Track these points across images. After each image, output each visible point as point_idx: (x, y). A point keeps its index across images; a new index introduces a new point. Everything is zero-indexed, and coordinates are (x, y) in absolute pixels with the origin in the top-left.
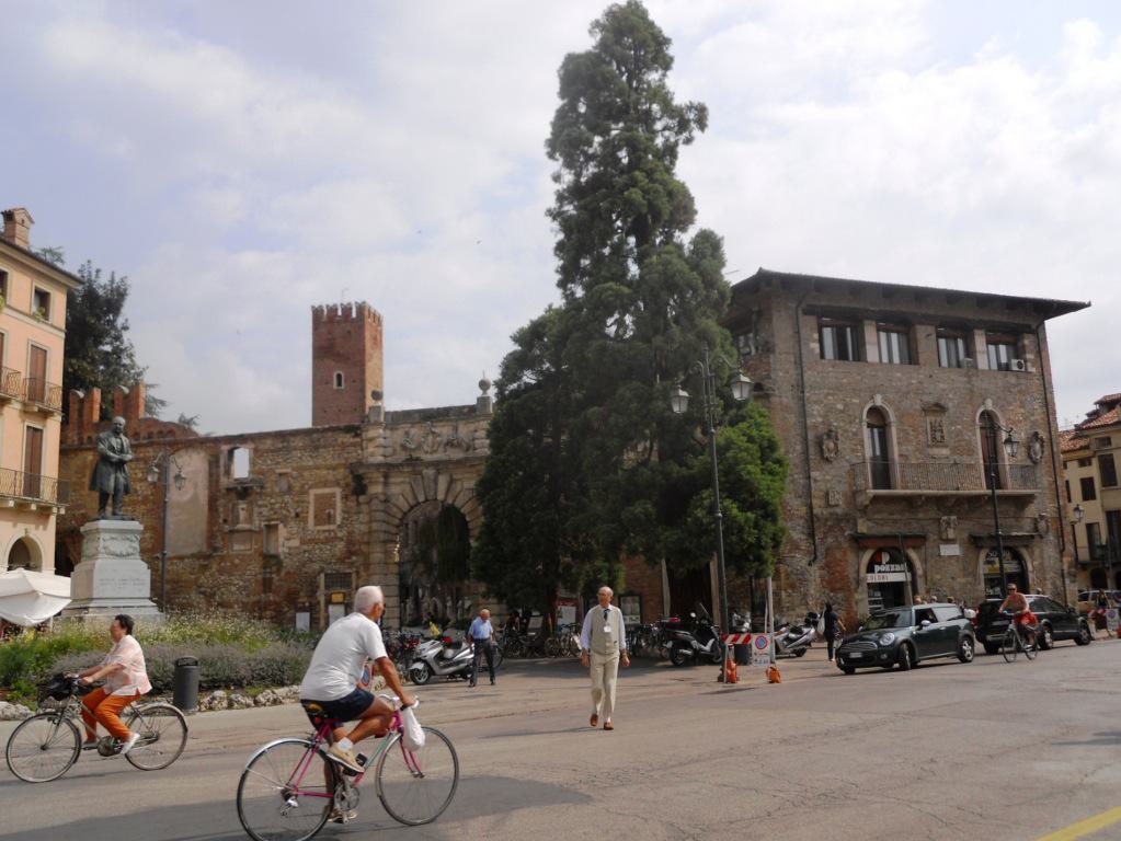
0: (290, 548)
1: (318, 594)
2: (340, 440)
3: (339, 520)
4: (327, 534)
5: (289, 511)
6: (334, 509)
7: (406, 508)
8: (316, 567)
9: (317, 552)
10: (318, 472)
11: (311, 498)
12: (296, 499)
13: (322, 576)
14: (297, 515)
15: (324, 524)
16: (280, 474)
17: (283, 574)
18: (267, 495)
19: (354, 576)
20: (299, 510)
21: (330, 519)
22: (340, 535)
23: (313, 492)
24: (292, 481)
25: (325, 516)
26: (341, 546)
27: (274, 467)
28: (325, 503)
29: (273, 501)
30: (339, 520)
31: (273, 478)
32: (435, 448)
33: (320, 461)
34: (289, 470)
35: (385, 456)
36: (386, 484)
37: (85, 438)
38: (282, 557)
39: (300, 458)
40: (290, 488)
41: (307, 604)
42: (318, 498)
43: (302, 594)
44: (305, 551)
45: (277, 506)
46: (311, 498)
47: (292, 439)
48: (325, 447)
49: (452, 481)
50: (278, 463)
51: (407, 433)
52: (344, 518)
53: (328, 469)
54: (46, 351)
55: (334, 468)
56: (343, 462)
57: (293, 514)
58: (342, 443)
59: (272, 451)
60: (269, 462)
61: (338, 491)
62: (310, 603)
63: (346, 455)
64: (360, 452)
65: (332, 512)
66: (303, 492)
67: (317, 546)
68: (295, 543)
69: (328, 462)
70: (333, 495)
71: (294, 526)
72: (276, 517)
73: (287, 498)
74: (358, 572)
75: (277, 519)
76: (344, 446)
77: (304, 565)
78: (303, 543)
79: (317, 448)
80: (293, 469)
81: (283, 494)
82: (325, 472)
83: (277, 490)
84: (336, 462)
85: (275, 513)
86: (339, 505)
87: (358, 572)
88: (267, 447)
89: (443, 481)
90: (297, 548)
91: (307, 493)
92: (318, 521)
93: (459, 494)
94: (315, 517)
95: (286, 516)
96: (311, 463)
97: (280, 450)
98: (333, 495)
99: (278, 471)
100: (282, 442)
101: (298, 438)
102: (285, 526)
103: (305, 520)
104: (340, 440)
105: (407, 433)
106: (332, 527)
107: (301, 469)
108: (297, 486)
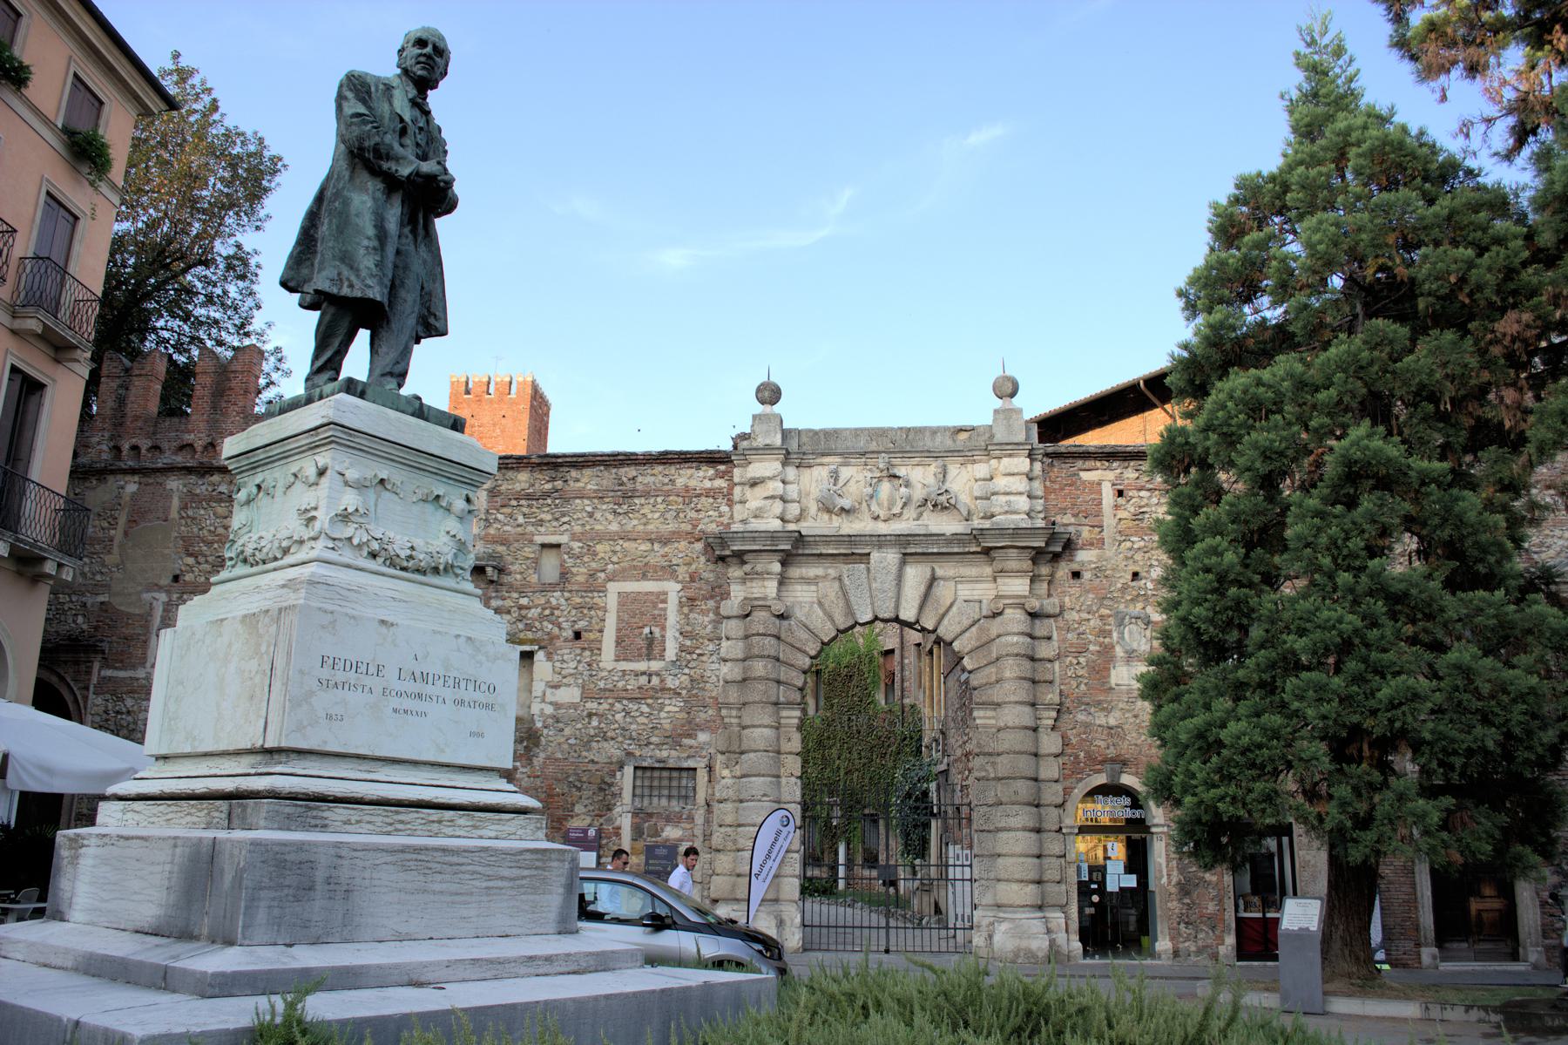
0: (557, 706)
1: (618, 809)
2: (680, 482)
3: (671, 652)
4: (643, 680)
5: (560, 628)
6: (663, 628)
7: (827, 633)
8: (612, 750)
9: (619, 717)
10: (626, 545)
11: (612, 601)
12: (578, 600)
13: (629, 770)
14: (578, 635)
15: (638, 657)
16: (544, 546)
17: (537, 762)
18: (511, 588)
19: (702, 776)
20: (581, 625)
21: (651, 648)
22: (671, 683)
23: (614, 588)
24: (570, 562)
25: (642, 643)
26: (673, 707)
27: (530, 528)
28: (640, 612)
29: (524, 601)
30: (671, 652)
31: (528, 551)
32: (896, 510)
33: (633, 523)
34: (564, 539)
35: (782, 520)
36: (783, 581)
37: (126, 446)
38: (539, 725)
39: (591, 515)
40: (565, 575)
41: (592, 832)
42: (624, 598)
43: (578, 808)
44: (590, 715)
45: (534, 613)
46: (612, 601)
47: (574, 473)
48: (646, 494)
49: (933, 580)
50: (541, 522)
51: (835, 476)
52: (682, 649)
53: (652, 541)
54: (76, 218)
55: (665, 541)
56: (689, 528)
57: (569, 634)
58: (687, 489)
59: (529, 497)
60: (521, 520)
61: (672, 588)
62: (599, 831)
63: (693, 514)
64: (724, 509)
65: (657, 631)
66: (593, 586)
67: (618, 706)
68: (570, 695)
69: (650, 527)
70: (662, 597)
71: (569, 657)
72: (530, 635)
73: (556, 598)
74: (710, 768)
75: (532, 642)
76: (689, 495)
77: (587, 745)
78: (586, 696)
79: (628, 496)
80: (574, 537)
81: (546, 588)
82: (645, 546)
83: (534, 578)
84: (672, 527)
85: (529, 627)
86: (673, 617)
87: (710, 768)
88: (518, 487)
89: (915, 575)
90: (575, 706)
91: (602, 590)
92: (624, 649)
93: (951, 605)
94: (618, 642)
95: (552, 638)
96: (614, 527)
97: (546, 495)
98: (662, 597)
99: (539, 539)
100: (553, 479)
101: (588, 472)
102: (549, 657)
103: (595, 648)
104: (680, 482)
105: (835, 476)
106: (655, 665)
107: (590, 539)
108: (580, 574)
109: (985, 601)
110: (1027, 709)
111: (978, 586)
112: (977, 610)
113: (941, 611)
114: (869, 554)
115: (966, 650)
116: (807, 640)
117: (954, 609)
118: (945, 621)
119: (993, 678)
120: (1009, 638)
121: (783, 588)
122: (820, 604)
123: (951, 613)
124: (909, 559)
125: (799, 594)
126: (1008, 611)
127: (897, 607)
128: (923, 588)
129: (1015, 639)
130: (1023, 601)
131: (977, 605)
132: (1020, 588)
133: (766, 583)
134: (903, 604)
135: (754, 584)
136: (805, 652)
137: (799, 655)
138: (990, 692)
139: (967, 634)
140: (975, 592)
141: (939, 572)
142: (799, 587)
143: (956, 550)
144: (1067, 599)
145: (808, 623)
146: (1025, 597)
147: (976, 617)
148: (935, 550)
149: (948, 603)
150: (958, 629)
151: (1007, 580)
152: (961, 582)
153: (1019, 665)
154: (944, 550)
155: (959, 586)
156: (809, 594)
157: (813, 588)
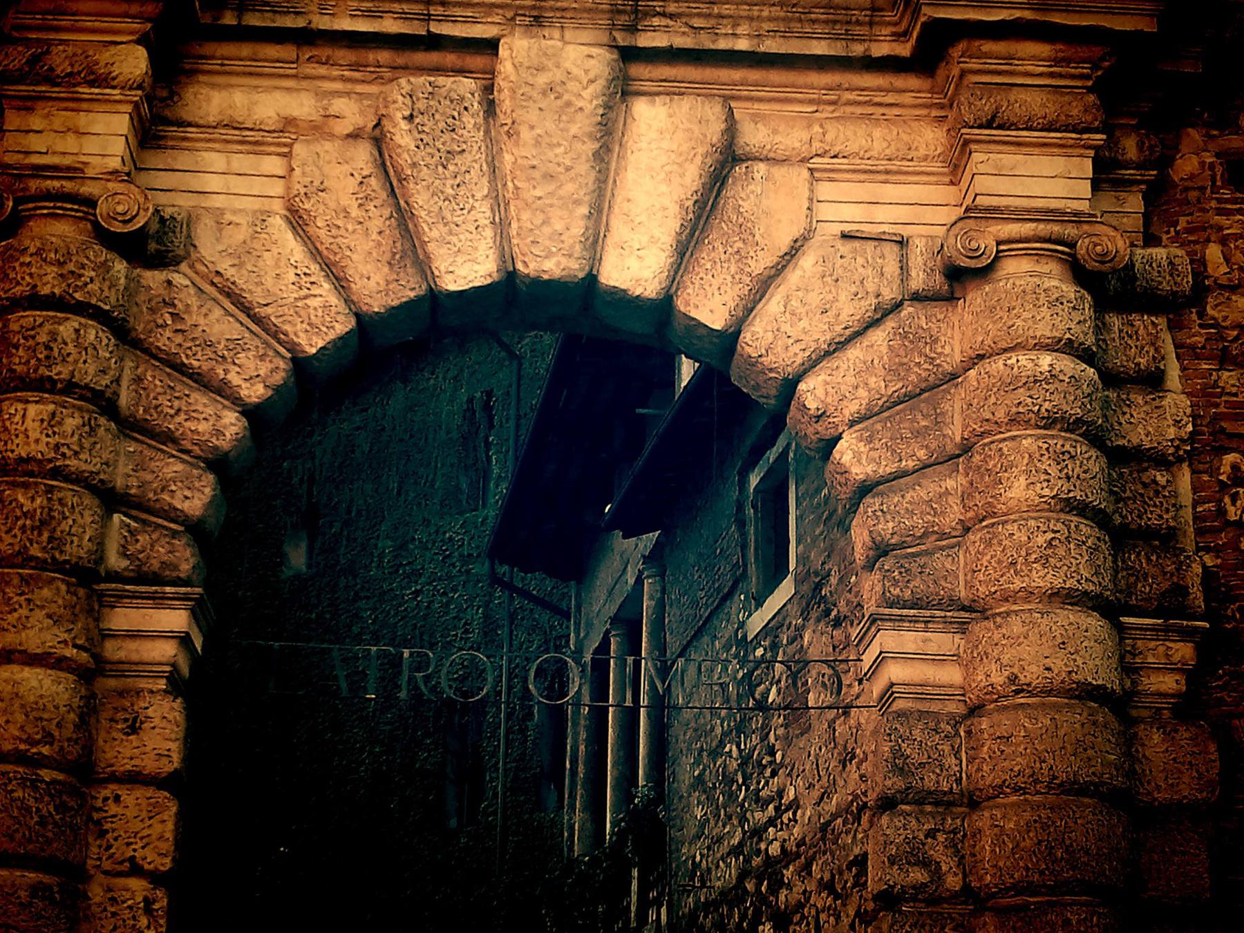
109: (918, 248)
110: (1094, 623)
111: (891, 192)
112: (892, 268)
113: (761, 263)
114: (491, 46)
115: (851, 408)
116: (236, 345)
117: (808, 262)
118: (773, 305)
119: (954, 514)
120: (1022, 360)
121: (155, 159)
122: (297, 221)
123: (793, 277)
124: (637, 70)
125: (213, 183)
126: (1016, 269)
127: (595, 243)
128: (692, 178)
129: (1046, 360)
130: (1070, 231)
131: (891, 251)
132: (1059, 188)
133: (82, 120)
134: (619, 230)
135: (36, 122)
136: (222, 390)
137: (200, 400)
138: (941, 562)
139: (854, 353)
140: (881, 214)
141: (753, 136)
142: (215, 160)
143: (819, 48)
144: (1214, 252)
145: (241, 280)
146: (1077, 218)
147: (890, 293)
148: (743, 45)
149: (784, 243)
150: (818, 333)
151: (1009, 159)
152: (832, 175)
153: (1060, 457)
154: (771, 46)
155: (825, 190)
156: (258, 186)
157: (273, 165)
